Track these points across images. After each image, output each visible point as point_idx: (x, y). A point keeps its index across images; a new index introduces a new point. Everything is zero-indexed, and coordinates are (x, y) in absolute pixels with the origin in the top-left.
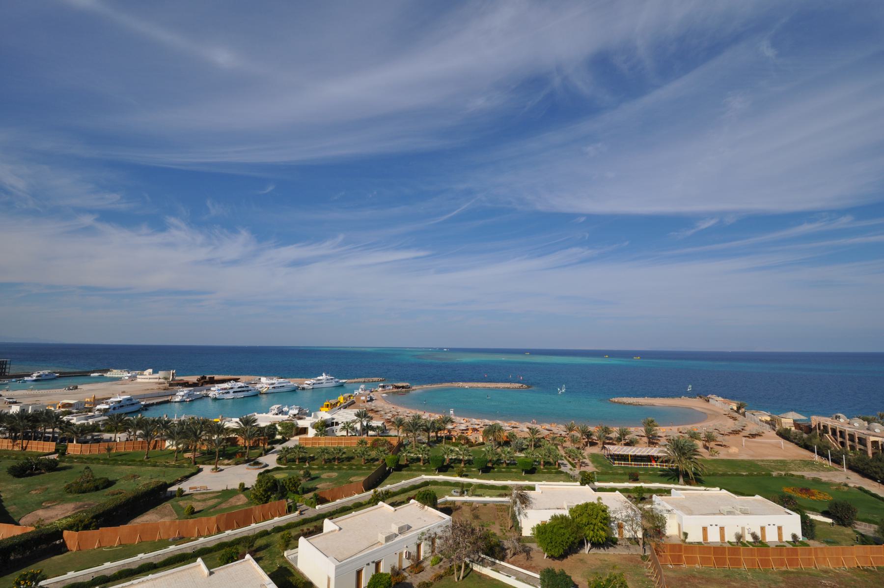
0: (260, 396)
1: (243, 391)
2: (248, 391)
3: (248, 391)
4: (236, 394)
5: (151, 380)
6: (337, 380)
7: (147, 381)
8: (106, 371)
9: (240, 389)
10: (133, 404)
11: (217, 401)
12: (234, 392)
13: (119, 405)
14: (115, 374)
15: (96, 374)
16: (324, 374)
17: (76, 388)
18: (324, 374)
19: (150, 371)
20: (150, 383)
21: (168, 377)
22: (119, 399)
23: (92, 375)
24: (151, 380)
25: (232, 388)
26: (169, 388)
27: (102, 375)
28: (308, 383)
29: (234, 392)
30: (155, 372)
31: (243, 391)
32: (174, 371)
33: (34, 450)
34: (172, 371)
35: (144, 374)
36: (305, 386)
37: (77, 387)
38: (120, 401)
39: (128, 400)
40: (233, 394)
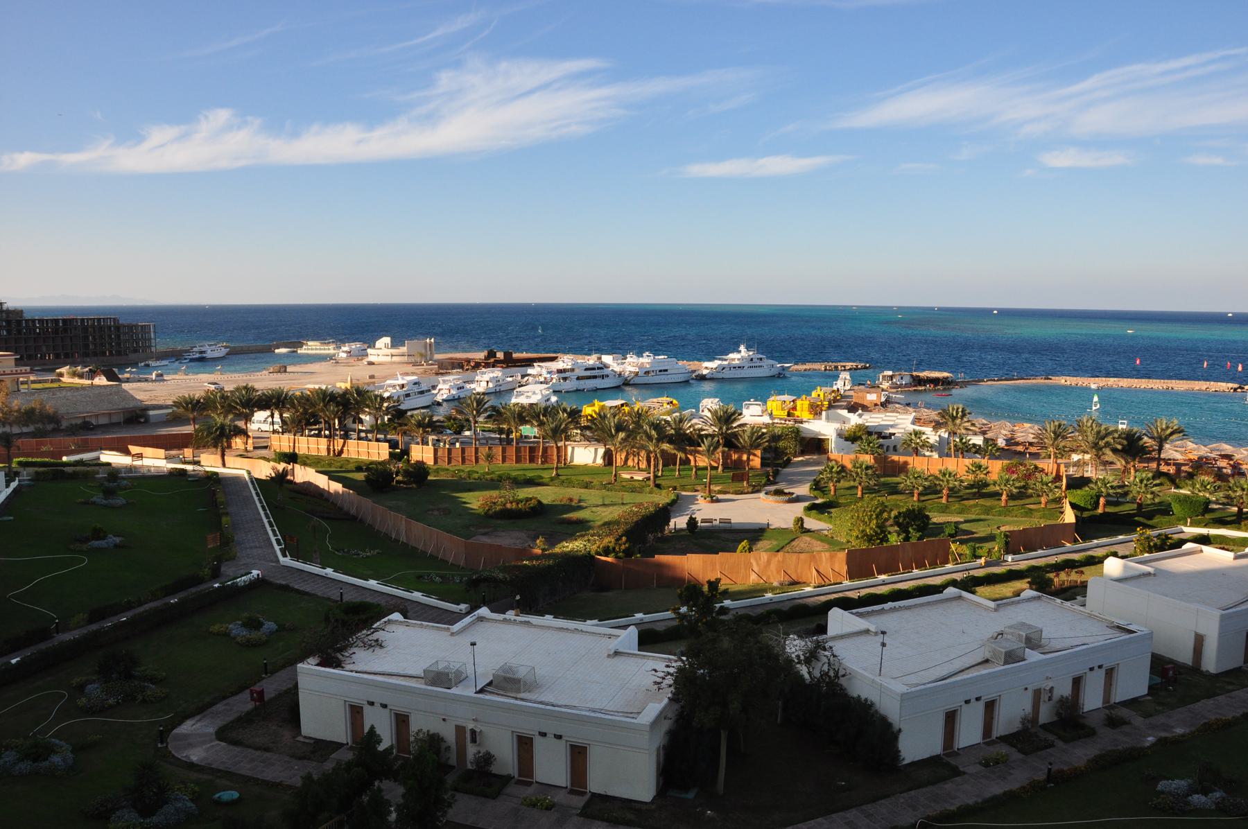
0: (627, 389)
1: (595, 377)
2: (603, 377)
3: (603, 377)
4: (582, 382)
5: (395, 359)
6: (771, 362)
7: (388, 359)
8: (300, 345)
9: (588, 373)
10: (422, 392)
11: (579, 392)
12: (578, 378)
13: (416, 389)
14: (312, 349)
15: (283, 350)
16: (742, 348)
17: (285, 371)
18: (742, 348)
19: (387, 340)
20: (394, 363)
21: (423, 351)
22: (401, 382)
23: (277, 351)
24: (395, 359)
25: (572, 370)
26: (441, 371)
27: (294, 352)
28: (708, 367)
29: (578, 378)
30: (394, 345)
31: (595, 377)
32: (432, 340)
33: (354, 456)
34: (428, 340)
35: (376, 347)
36: (705, 372)
37: (286, 367)
38: (403, 386)
39: (415, 384)
40: (577, 382)
